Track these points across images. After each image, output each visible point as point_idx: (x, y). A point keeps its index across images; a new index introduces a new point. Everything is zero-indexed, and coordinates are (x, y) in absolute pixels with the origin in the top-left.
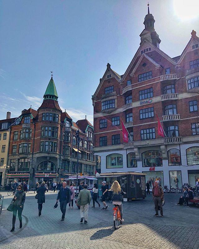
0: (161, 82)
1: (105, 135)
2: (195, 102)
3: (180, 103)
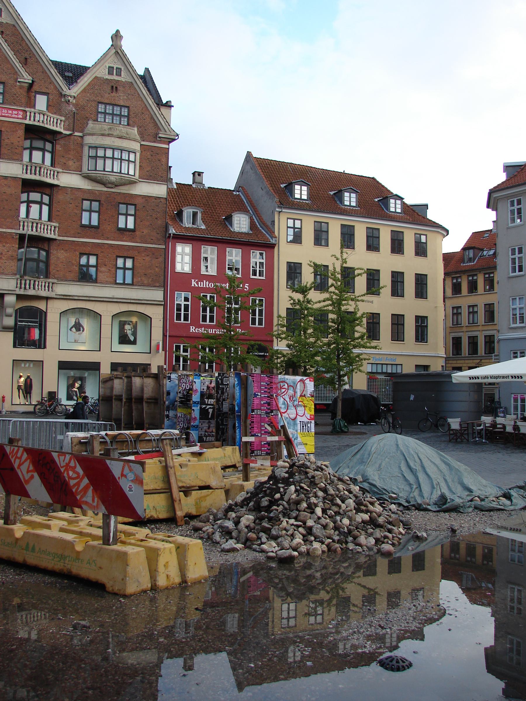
0: (26, 125)
2: (95, 205)
3: (59, 197)
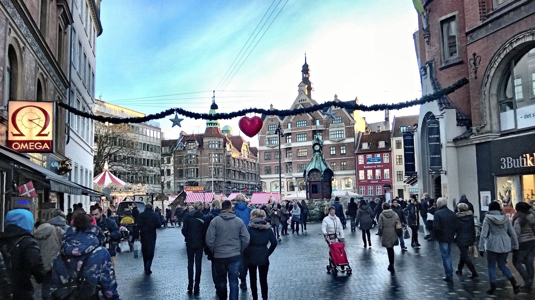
1: (269, 166)
